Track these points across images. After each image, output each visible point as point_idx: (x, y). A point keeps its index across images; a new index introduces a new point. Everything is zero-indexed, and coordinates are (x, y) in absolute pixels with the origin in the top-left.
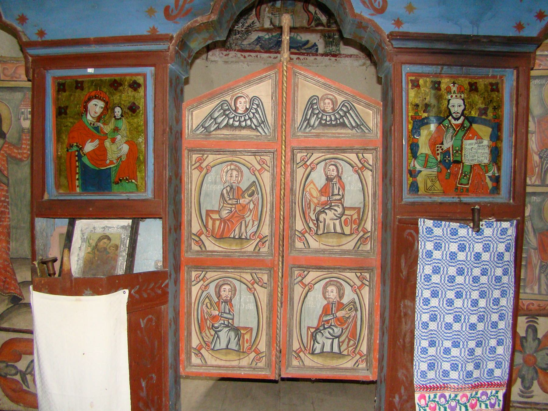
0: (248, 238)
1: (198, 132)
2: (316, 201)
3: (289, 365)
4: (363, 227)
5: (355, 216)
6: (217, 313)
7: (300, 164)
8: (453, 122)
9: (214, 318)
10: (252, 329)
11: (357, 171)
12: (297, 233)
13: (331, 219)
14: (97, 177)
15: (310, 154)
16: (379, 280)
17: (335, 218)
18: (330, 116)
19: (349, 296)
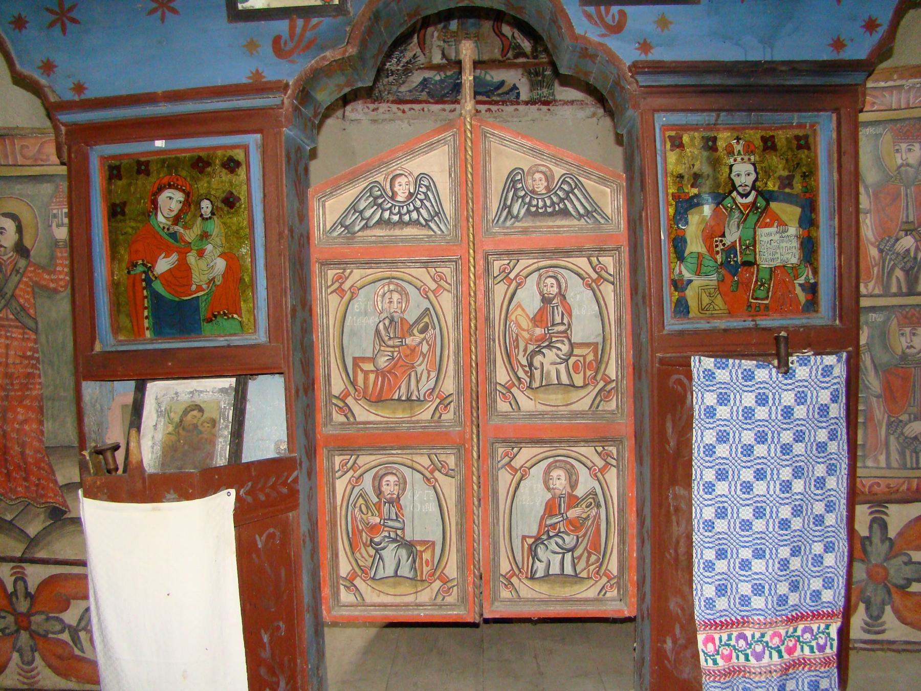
0: (422, 398)
1: (335, 234)
2: (527, 336)
3: (495, 598)
4: (604, 374)
5: (590, 357)
6: (378, 520)
7: (499, 278)
8: (739, 200)
9: (373, 528)
10: (433, 543)
11: (589, 286)
12: (498, 388)
13: (551, 364)
14: (178, 314)
15: (513, 262)
16: (633, 458)
17: (559, 360)
18: (543, 200)
19: (586, 484)
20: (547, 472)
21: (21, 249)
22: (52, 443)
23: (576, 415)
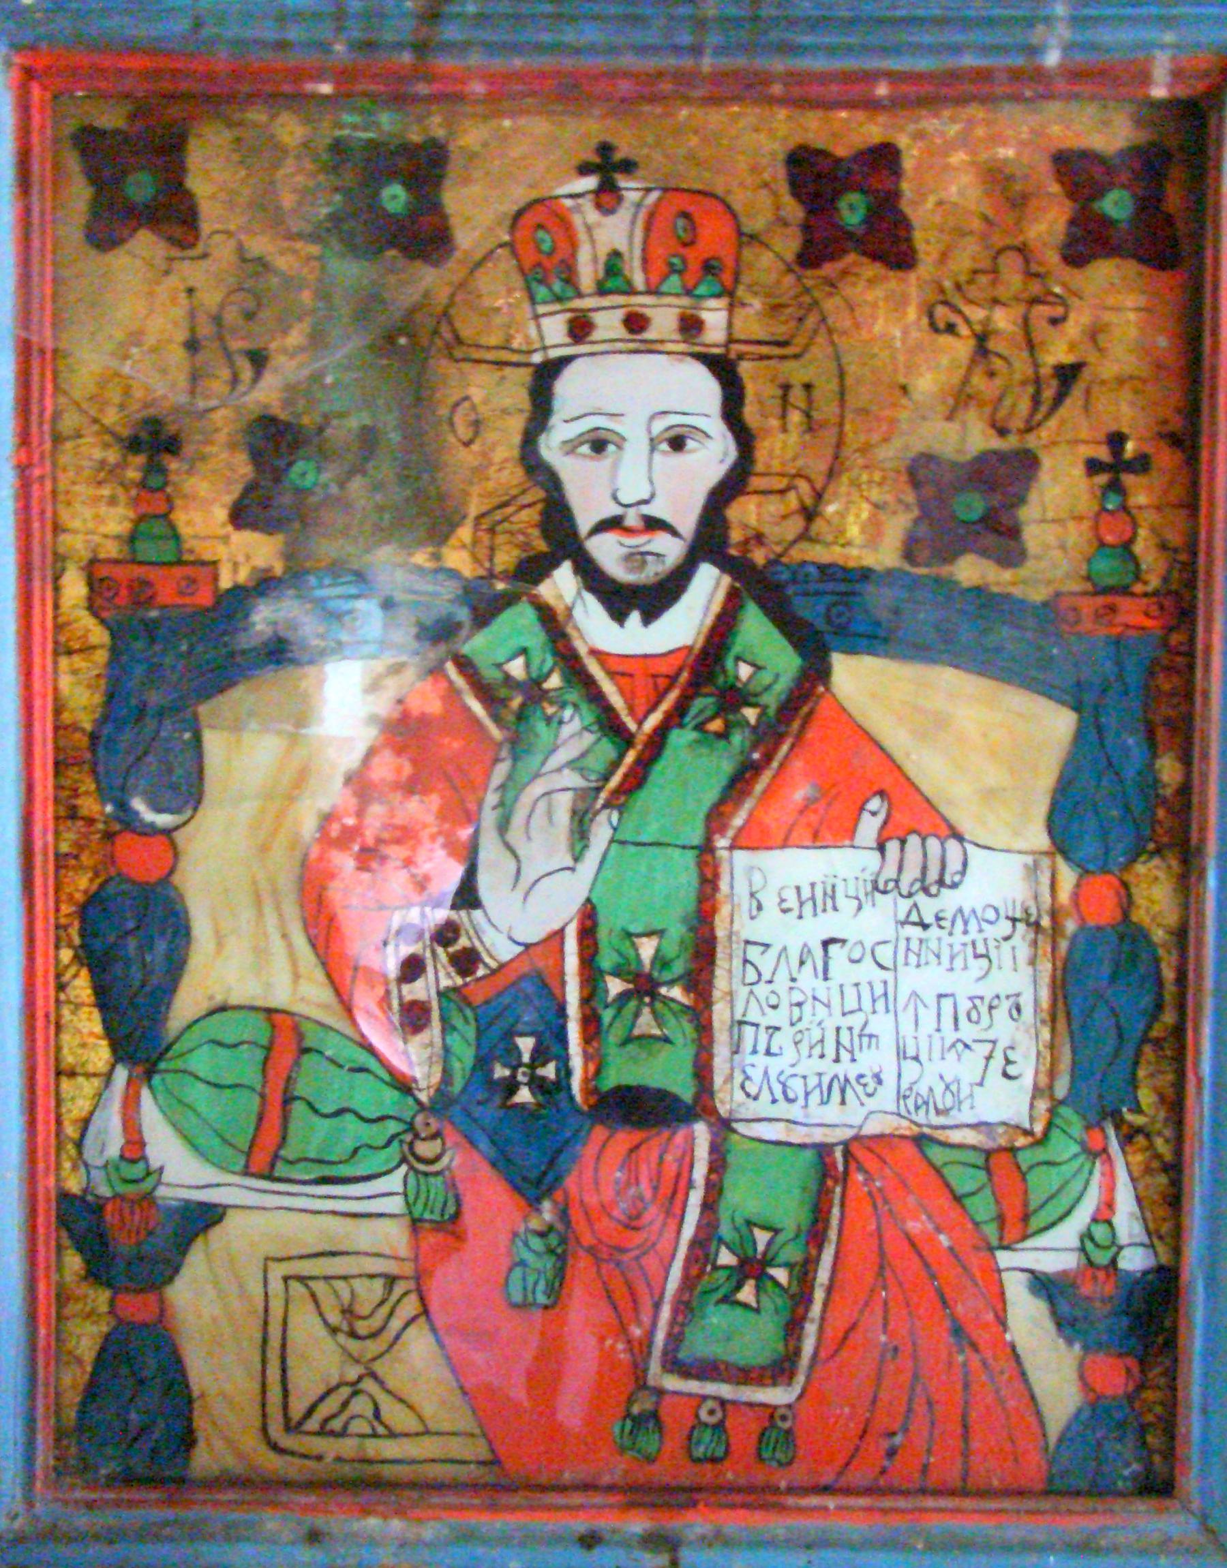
8: (595, 627)
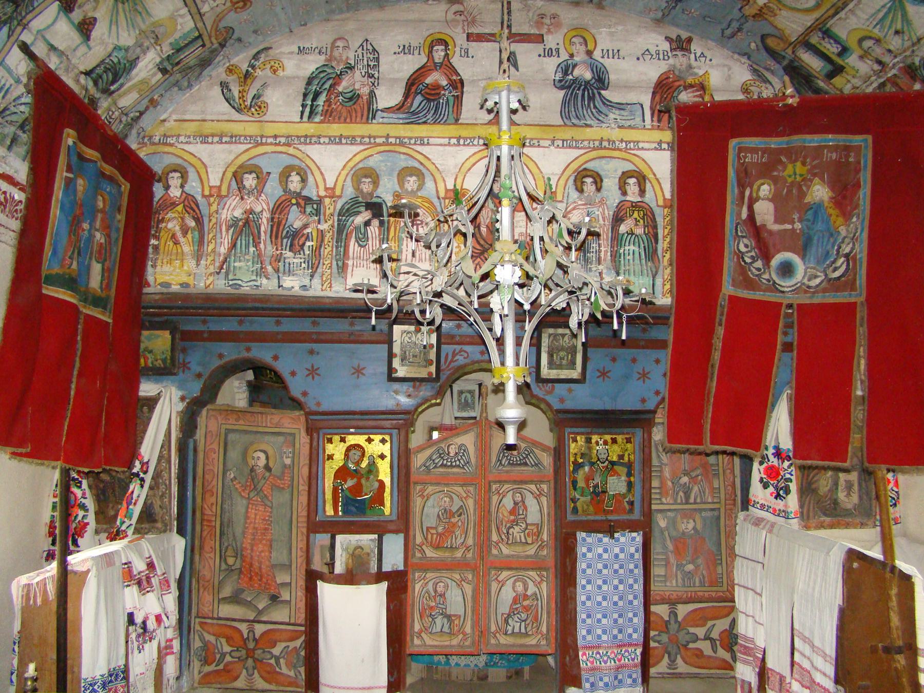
5: (535, 530)
9: (432, 608)
10: (460, 616)
20: (514, 583)
21: (267, 468)
22: (275, 563)
23: (528, 556)
